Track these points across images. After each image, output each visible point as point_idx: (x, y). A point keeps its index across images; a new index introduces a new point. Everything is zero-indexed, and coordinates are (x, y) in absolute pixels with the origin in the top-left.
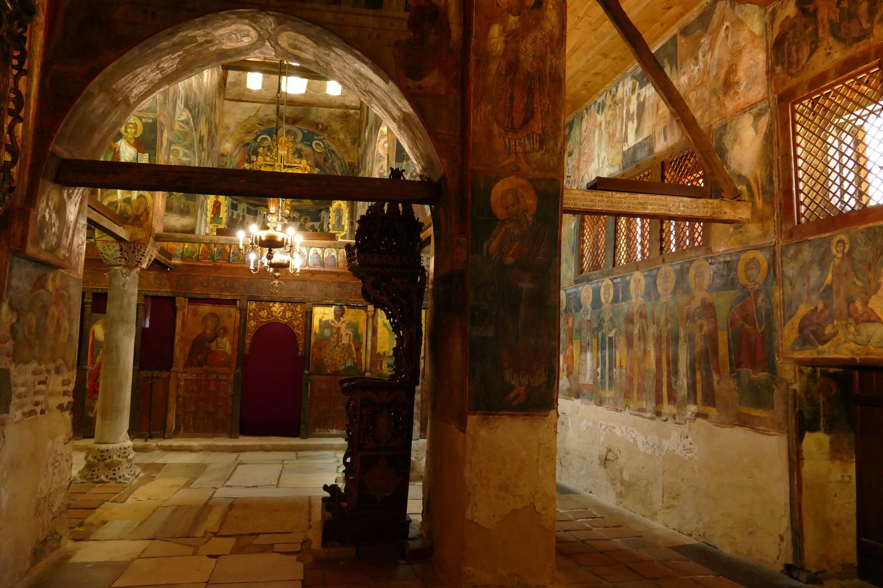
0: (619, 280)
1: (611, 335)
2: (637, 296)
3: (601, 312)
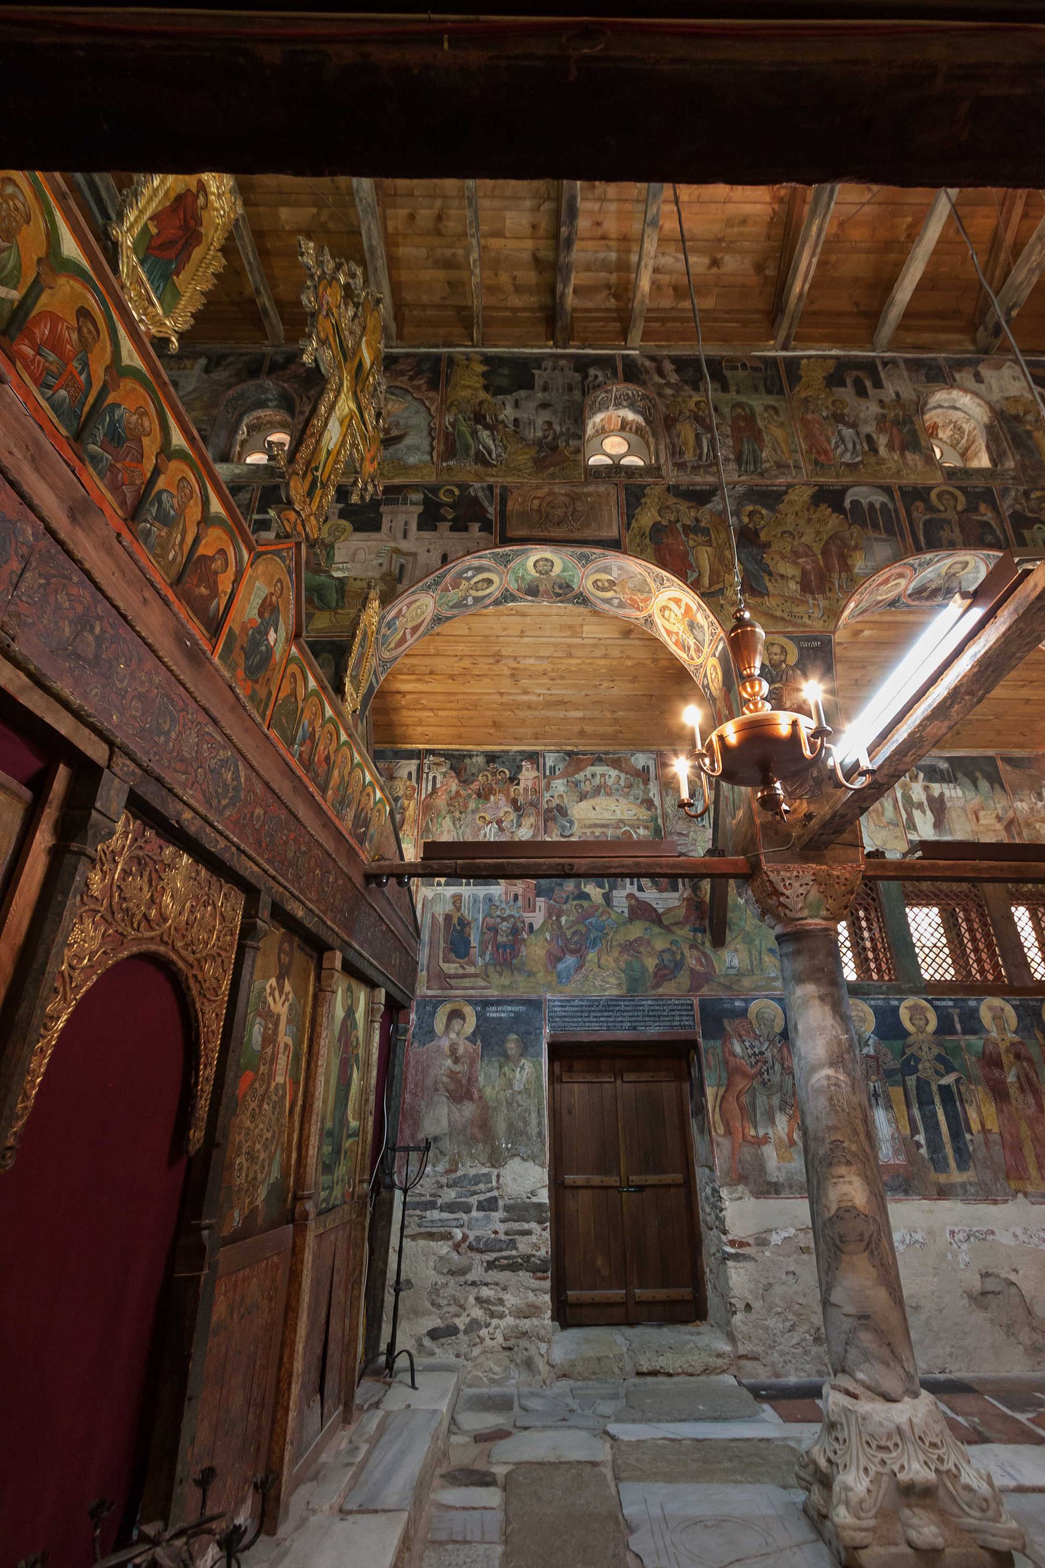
0: (951, 1003)
1: (949, 1079)
2: (1002, 1030)
3: (905, 1046)
